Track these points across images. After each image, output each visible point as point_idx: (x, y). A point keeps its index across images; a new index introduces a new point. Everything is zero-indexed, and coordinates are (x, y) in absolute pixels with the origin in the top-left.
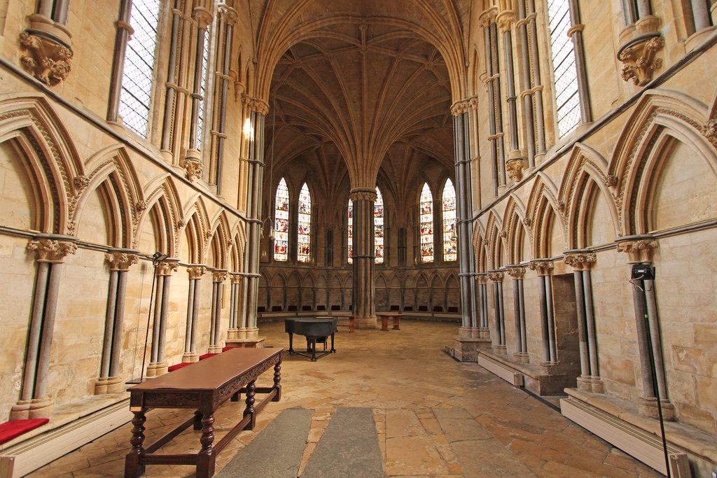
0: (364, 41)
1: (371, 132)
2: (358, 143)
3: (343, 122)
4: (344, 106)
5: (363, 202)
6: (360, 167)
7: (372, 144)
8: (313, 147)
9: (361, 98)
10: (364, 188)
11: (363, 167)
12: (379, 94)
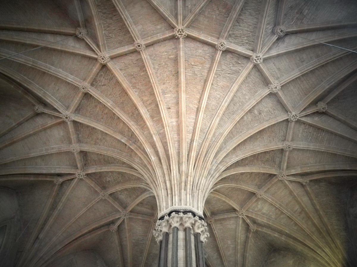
0: (180, 18)
1: (192, 141)
2: (172, 152)
3: (153, 130)
4: (156, 114)
5: (181, 235)
6: (175, 182)
7: (193, 154)
8: (113, 222)
9: (178, 103)
10: (183, 207)
11: (180, 184)
12: (200, 98)
